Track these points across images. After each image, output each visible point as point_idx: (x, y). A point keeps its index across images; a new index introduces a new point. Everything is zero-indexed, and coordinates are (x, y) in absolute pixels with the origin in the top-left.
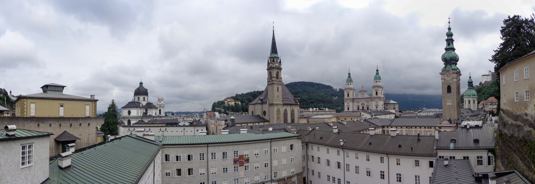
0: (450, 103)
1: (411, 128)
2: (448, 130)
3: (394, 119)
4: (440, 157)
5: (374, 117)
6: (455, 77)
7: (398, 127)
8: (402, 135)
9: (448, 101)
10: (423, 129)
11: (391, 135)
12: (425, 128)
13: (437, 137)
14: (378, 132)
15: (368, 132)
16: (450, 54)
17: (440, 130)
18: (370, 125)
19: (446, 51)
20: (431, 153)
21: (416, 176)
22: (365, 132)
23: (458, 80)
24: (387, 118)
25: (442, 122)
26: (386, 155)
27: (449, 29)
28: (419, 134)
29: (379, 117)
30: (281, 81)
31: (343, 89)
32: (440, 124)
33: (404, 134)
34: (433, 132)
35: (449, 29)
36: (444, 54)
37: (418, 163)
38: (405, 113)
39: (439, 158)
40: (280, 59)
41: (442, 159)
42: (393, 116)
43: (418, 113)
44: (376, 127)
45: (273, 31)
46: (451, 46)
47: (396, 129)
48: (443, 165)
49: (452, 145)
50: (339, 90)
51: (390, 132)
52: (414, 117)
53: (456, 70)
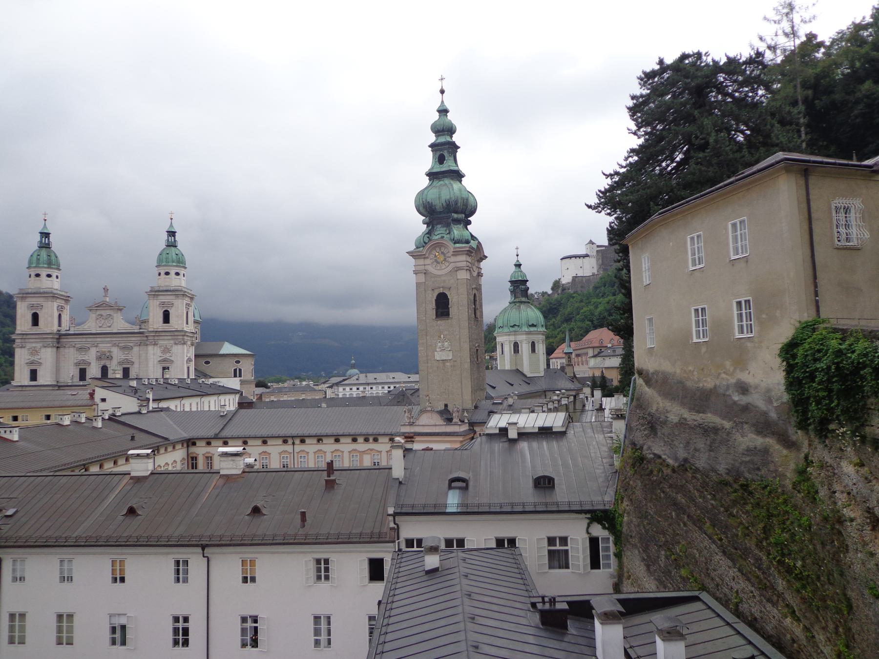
1: (303, 441)
2: (439, 446)
3: (235, 413)
4: (410, 543)
5: (152, 405)
6: (464, 264)
7: (250, 442)
8: (266, 471)
9: (439, 344)
10: (346, 446)
11: (222, 472)
12: (355, 440)
13: (398, 472)
14: (167, 464)
15: (122, 468)
16: (447, 191)
17: (408, 446)
18: (133, 438)
19: (430, 180)
20: (377, 531)
21: (317, 619)
22: (108, 466)
23: (475, 274)
24: (206, 409)
25: (417, 419)
26: (199, 550)
27: (443, 111)
28: (330, 465)
29: (172, 405)
31: (11, 293)
32: (411, 424)
33: (275, 464)
34: (384, 454)
35: (443, 111)
36: (422, 192)
37: (327, 570)
38: (280, 391)
39: (407, 547)
41: (415, 549)
42: (230, 403)
43: (331, 387)
44: (160, 444)
46: (448, 165)
47: (240, 449)
48: (421, 569)
49: (453, 500)
51: (216, 461)
52: (315, 404)
53: (467, 242)
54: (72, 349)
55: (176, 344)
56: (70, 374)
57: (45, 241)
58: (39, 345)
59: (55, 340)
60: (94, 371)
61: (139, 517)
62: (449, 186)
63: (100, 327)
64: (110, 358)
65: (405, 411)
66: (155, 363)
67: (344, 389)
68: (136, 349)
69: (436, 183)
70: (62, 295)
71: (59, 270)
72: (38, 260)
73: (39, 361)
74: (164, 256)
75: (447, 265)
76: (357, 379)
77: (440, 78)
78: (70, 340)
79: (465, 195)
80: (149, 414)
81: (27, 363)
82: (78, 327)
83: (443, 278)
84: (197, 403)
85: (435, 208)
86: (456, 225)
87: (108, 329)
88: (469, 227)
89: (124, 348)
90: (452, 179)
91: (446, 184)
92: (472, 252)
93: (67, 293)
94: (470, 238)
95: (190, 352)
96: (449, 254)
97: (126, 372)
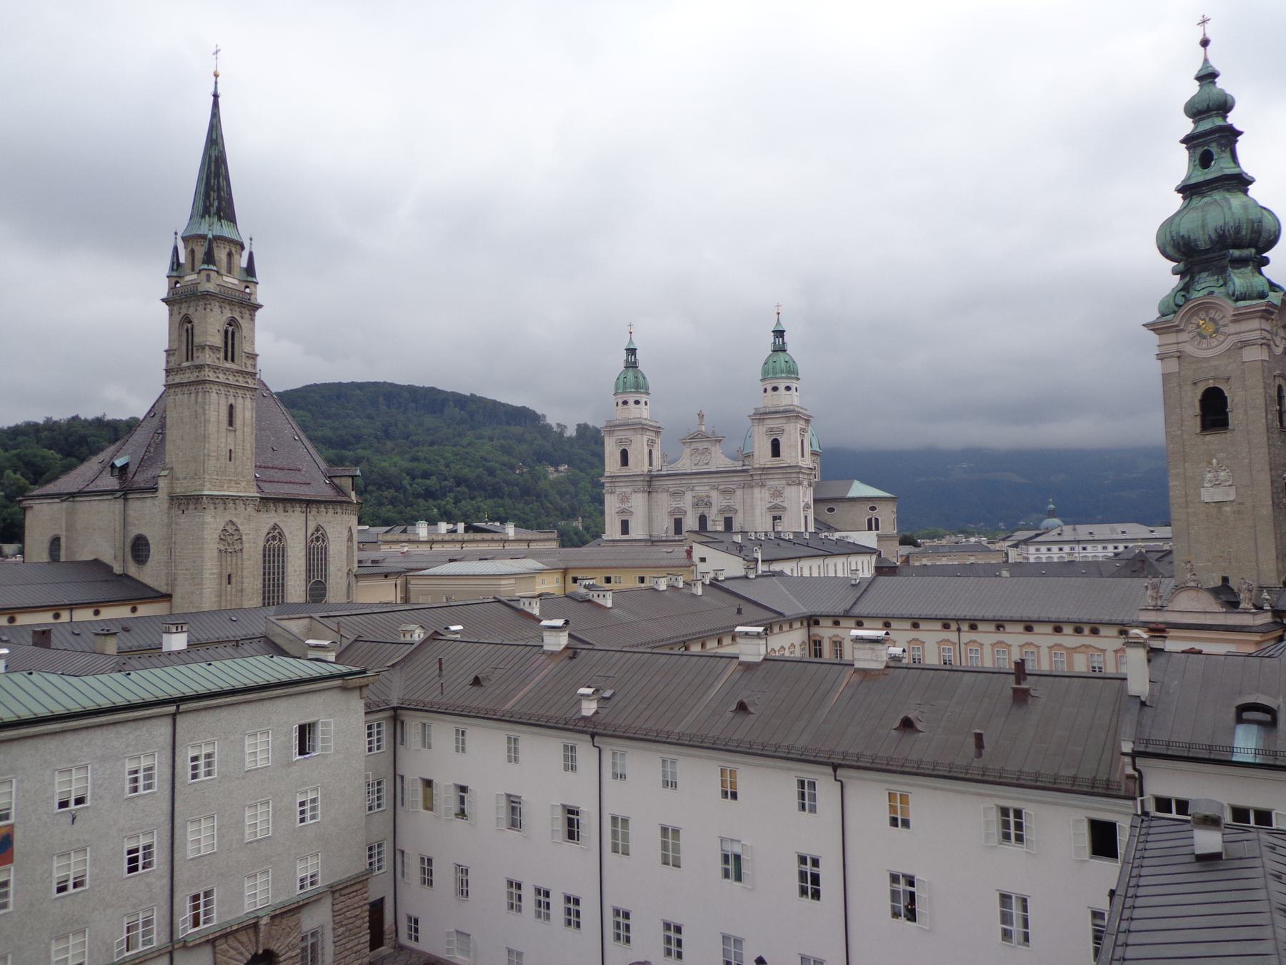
0: (1221, 489)
1: (973, 627)
2: (1214, 647)
3: (872, 581)
4: (1163, 804)
5: (761, 568)
6: (1257, 335)
7: (894, 625)
8: (918, 667)
9: (1209, 475)
10: (1043, 638)
11: (858, 665)
12: (1058, 630)
13: (1139, 684)
14: (783, 648)
15: (728, 649)
17: (1156, 644)
18: (739, 611)
19: (1184, 198)
20: (1102, 776)
21: (1005, 898)
22: (712, 645)
24: (832, 574)
25: (1170, 601)
26: (830, 770)
27: (1207, 77)
28: (1020, 665)
29: (787, 568)
30: (250, 369)
31: (598, 426)
32: (1159, 609)
33: (932, 659)
34: (1110, 657)
35: (1207, 77)
36: (1170, 220)
37: (1019, 826)
38: (937, 551)
39: (1158, 809)
40: (251, 255)
41: (1174, 815)
42: (864, 567)
43: (1015, 546)
44: (774, 621)
45: (216, 96)
46: (1221, 166)
47: (881, 633)
48: (1187, 850)
49: (1246, 742)
50: (574, 434)
51: (847, 647)
52: (991, 571)
53: (1262, 296)
54: (665, 494)
55: (788, 484)
56: (664, 525)
57: (631, 359)
58: (629, 490)
59: (646, 483)
60: (691, 523)
61: (751, 716)
62: (1224, 204)
63: (696, 465)
65: (1147, 587)
66: (764, 511)
67: (1038, 550)
68: (739, 492)
69: (1197, 202)
70: (651, 426)
71: (648, 394)
72: (625, 383)
74: (770, 364)
75: (1221, 340)
76: (1059, 534)
77: (1199, 19)
78: (662, 483)
79: (1254, 214)
80: (759, 580)
82: (671, 466)
84: (819, 566)
85: (1197, 246)
86: (1238, 268)
87: (706, 467)
88: (1264, 269)
89: (725, 492)
90: (1228, 191)
91: (1216, 201)
92: (1272, 313)
94: (1267, 288)
95: (805, 495)
96: (1225, 321)
97: (728, 523)
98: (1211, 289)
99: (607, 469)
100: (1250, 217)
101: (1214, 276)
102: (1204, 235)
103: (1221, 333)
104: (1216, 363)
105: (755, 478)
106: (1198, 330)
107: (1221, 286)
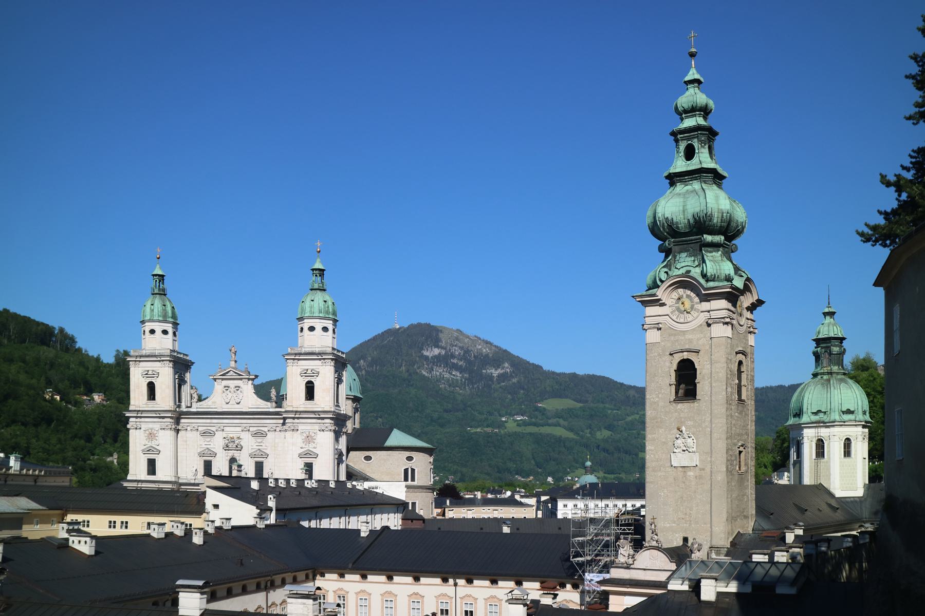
6: (724, 313)
58: (157, 426)
64: (239, 448)
73: (157, 447)
75: (695, 316)
81: (143, 451)
83: (689, 336)
85: (678, 227)
86: (711, 252)
89: (257, 434)
91: (695, 190)
93: (187, 355)
98: (688, 268)
99: (132, 402)
100: (720, 208)
101: (691, 256)
102: (684, 219)
103: (697, 310)
104: (690, 337)
105: (287, 421)
106: (677, 305)
107: (697, 266)
